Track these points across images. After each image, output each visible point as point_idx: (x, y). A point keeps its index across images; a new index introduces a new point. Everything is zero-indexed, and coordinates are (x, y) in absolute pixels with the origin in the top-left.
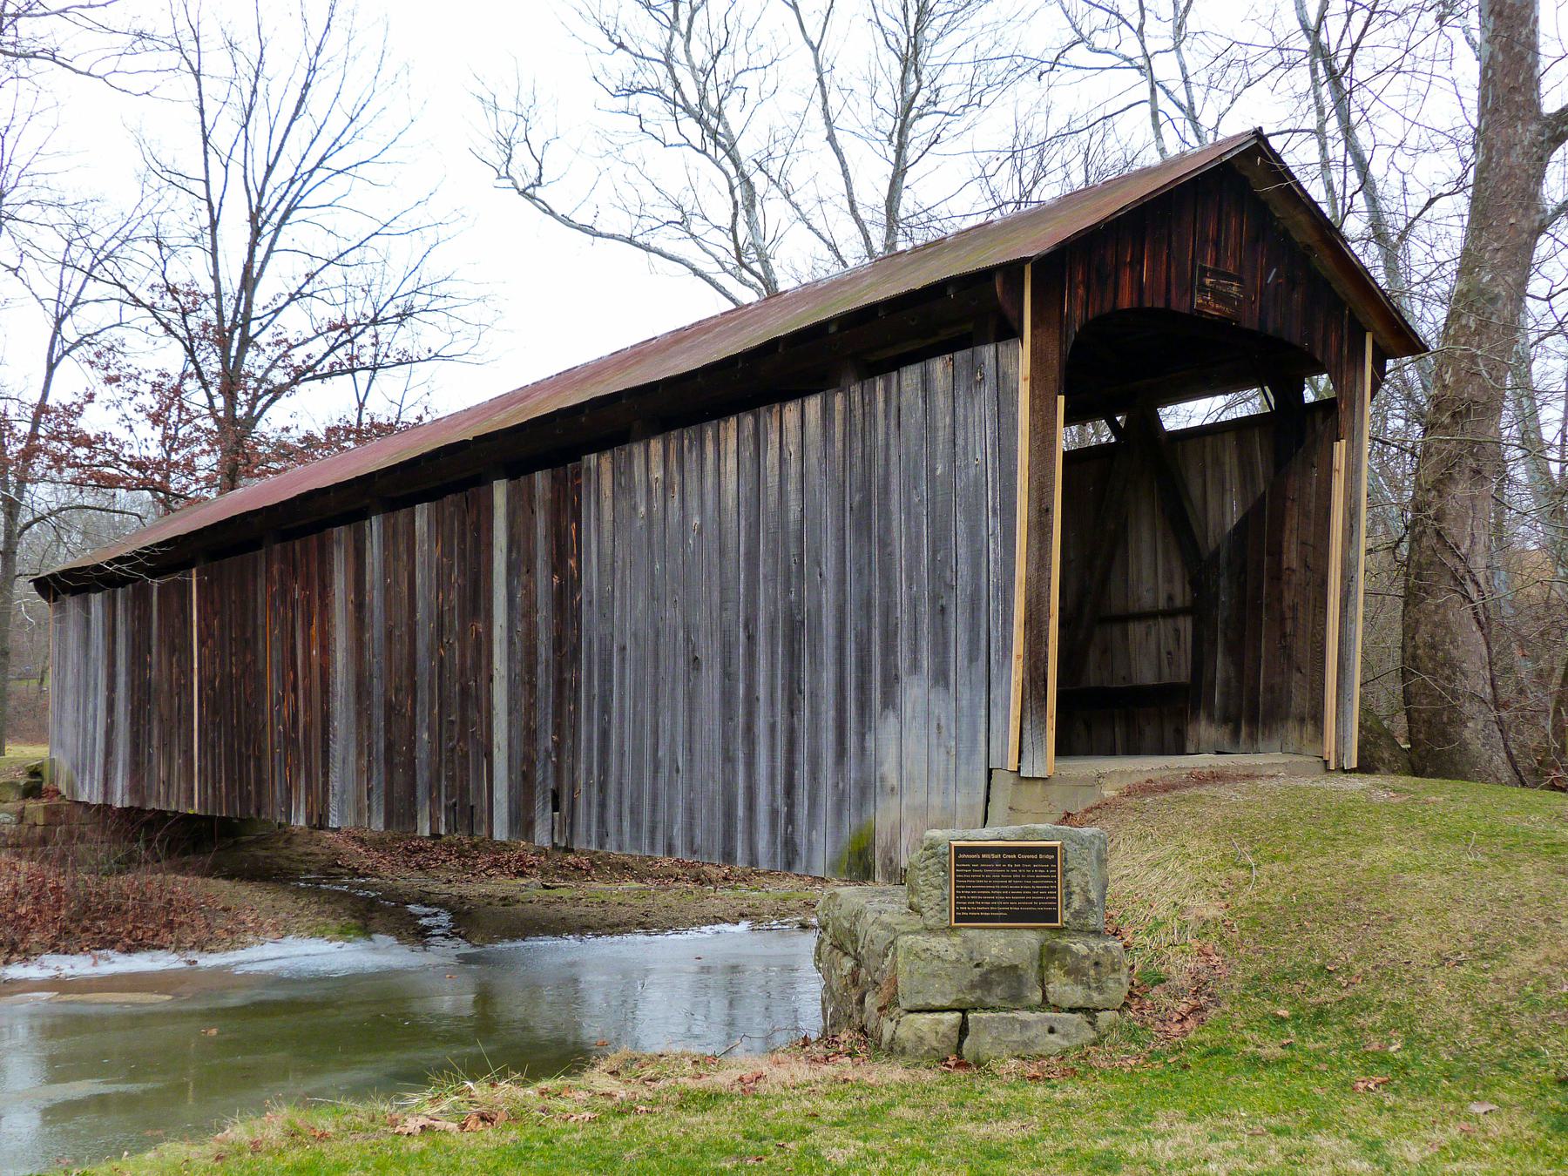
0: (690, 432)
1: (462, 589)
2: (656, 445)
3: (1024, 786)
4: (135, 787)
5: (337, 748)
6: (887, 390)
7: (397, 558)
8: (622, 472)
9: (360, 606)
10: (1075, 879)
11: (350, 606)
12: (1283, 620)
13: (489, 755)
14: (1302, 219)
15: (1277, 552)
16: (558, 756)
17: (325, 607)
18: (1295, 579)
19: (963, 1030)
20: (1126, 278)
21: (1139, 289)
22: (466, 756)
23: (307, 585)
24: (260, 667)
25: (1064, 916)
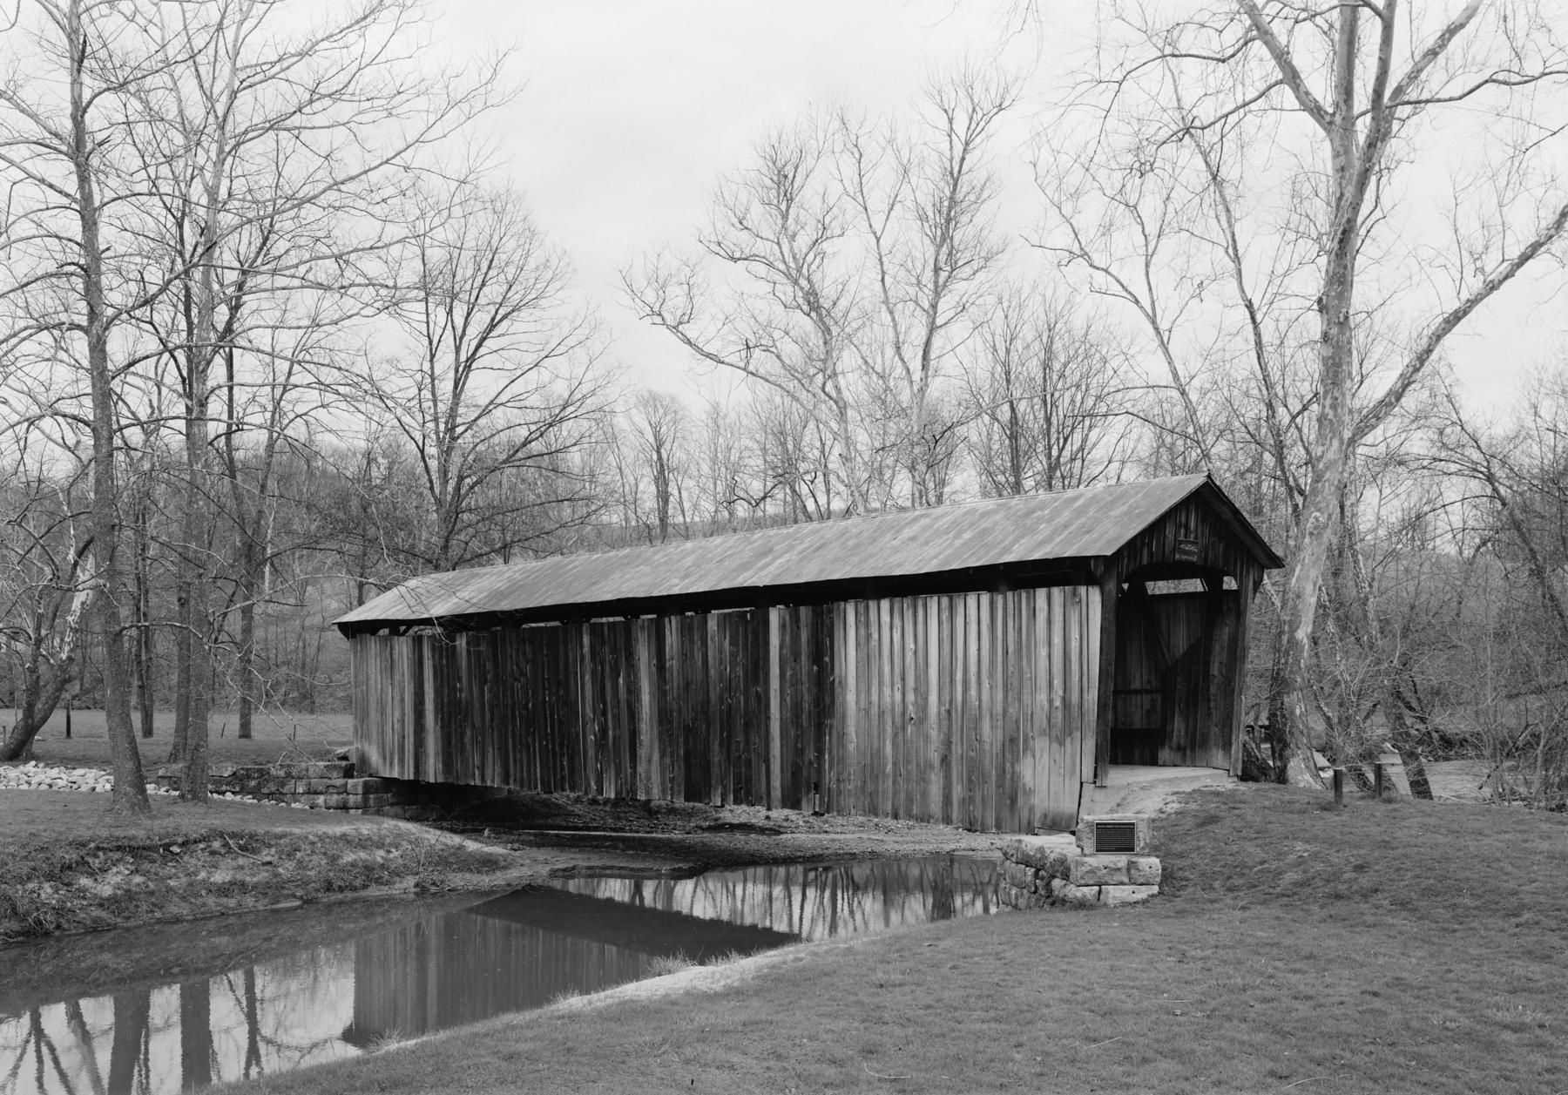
0: (907, 601)
1: (745, 667)
2: (885, 604)
3: (1098, 790)
4: (448, 765)
5: (643, 752)
6: (1028, 598)
7: (692, 642)
8: (863, 622)
9: (661, 667)
10: (1141, 834)
11: (654, 669)
12: (1209, 701)
13: (767, 762)
14: (1227, 511)
15: (1207, 664)
16: (819, 764)
17: (632, 667)
18: (1215, 681)
19: (1100, 892)
20: (1145, 553)
21: (1151, 553)
22: (749, 761)
23: (614, 650)
24: (573, 698)
25: (1137, 849)
